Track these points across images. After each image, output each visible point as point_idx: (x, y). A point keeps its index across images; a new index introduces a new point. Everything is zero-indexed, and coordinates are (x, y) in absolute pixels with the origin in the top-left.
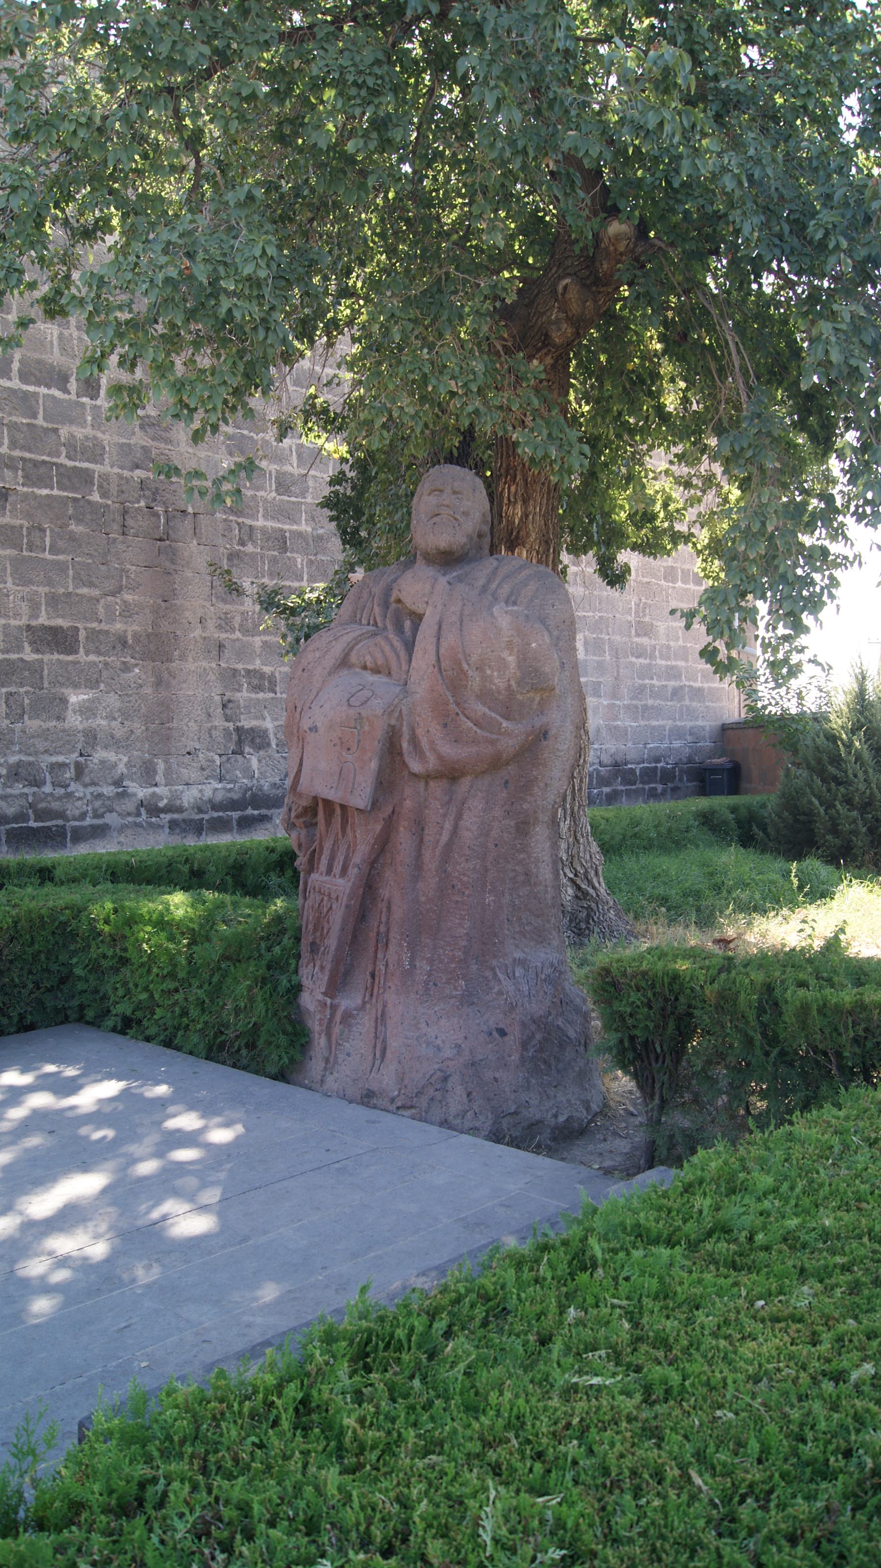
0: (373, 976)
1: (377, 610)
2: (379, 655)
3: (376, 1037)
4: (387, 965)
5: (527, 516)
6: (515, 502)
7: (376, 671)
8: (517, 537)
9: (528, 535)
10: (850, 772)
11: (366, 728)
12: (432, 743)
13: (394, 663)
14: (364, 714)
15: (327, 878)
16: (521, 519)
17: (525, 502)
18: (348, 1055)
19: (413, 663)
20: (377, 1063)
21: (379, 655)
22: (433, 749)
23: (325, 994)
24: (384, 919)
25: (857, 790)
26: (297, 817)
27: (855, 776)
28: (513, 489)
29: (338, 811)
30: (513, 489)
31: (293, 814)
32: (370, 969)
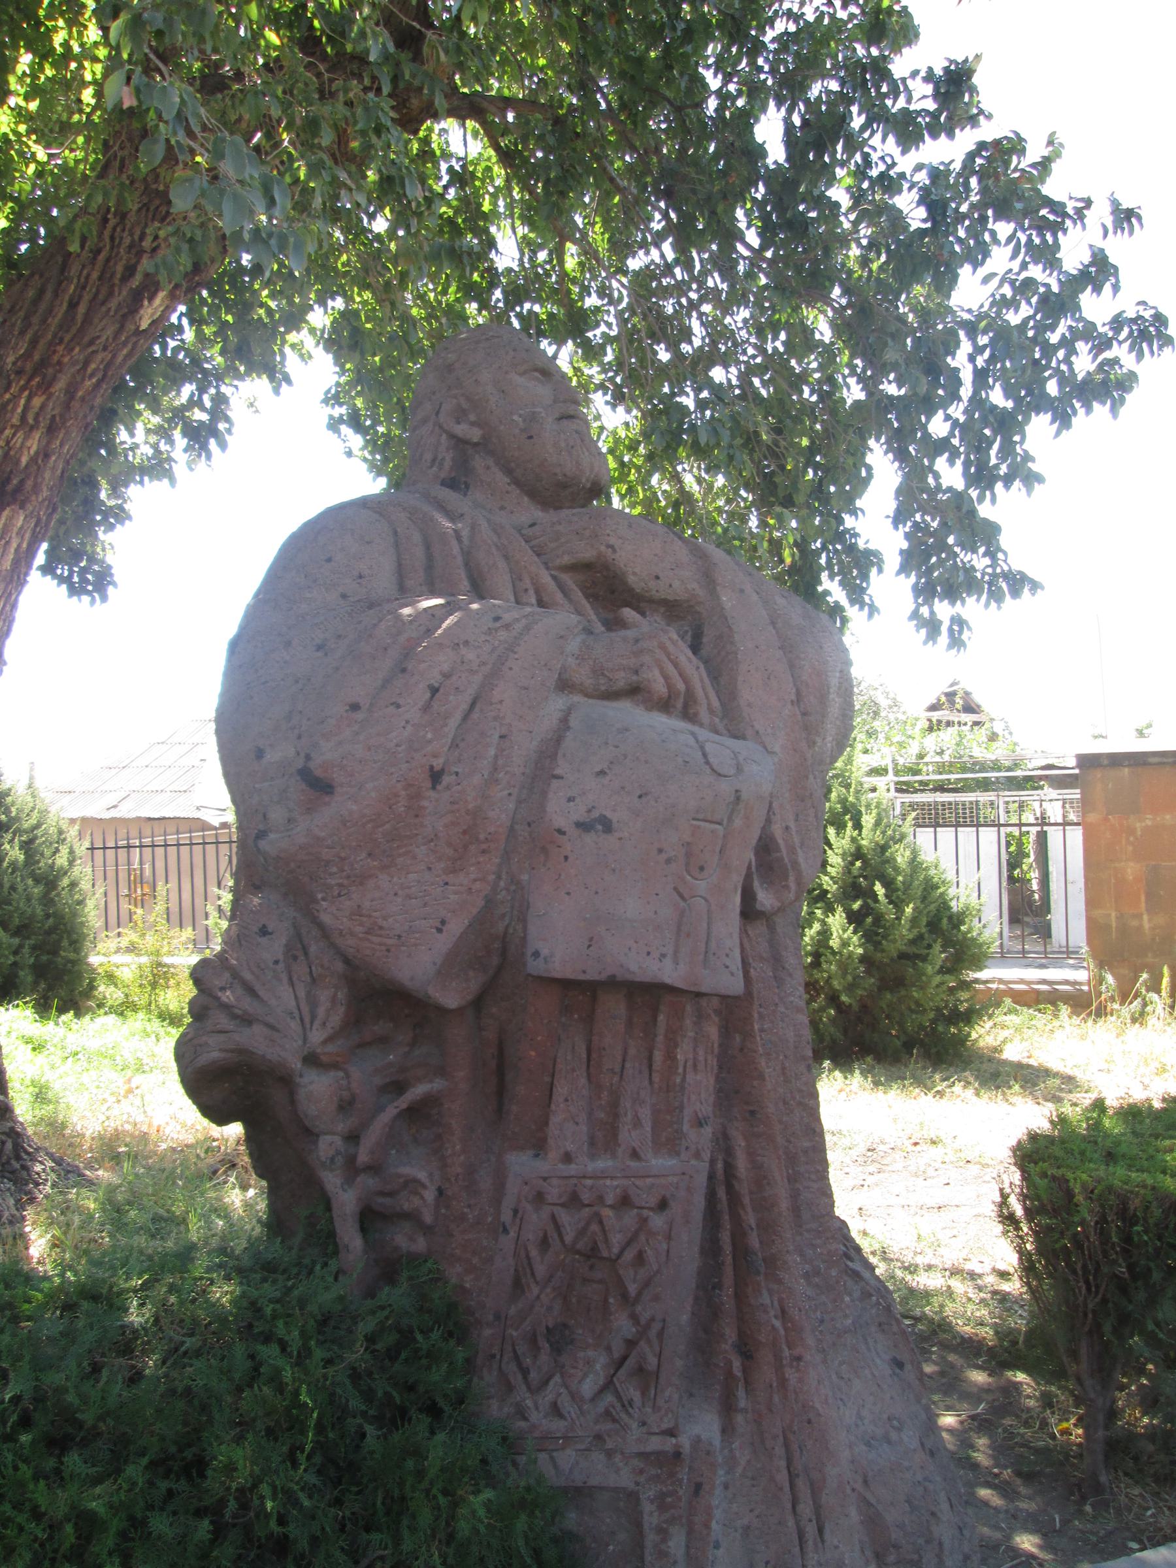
0: (746, 1351)
1: (546, 579)
2: (671, 670)
3: (792, 1477)
4: (784, 1313)
5: (47, 456)
6: (32, 428)
7: (665, 706)
8: (19, 489)
9: (36, 488)
10: (7, 885)
11: (738, 822)
12: (792, 850)
13: (699, 693)
14: (744, 796)
15: (603, 1163)
16: (33, 460)
17: (51, 430)
18: (717, 1546)
19: (746, 695)
20: (811, 1530)
21: (671, 670)
22: (795, 863)
23: (671, 1433)
24: (750, 1218)
25: (17, 908)
26: (326, 1042)
27: (13, 888)
28: (37, 402)
29: (614, 1007)
30: (37, 402)
31: (317, 1036)
32: (730, 1334)
